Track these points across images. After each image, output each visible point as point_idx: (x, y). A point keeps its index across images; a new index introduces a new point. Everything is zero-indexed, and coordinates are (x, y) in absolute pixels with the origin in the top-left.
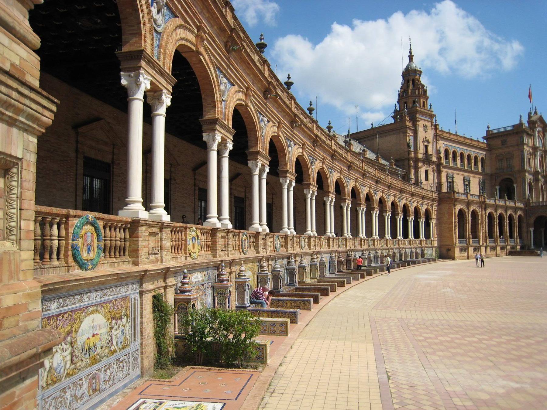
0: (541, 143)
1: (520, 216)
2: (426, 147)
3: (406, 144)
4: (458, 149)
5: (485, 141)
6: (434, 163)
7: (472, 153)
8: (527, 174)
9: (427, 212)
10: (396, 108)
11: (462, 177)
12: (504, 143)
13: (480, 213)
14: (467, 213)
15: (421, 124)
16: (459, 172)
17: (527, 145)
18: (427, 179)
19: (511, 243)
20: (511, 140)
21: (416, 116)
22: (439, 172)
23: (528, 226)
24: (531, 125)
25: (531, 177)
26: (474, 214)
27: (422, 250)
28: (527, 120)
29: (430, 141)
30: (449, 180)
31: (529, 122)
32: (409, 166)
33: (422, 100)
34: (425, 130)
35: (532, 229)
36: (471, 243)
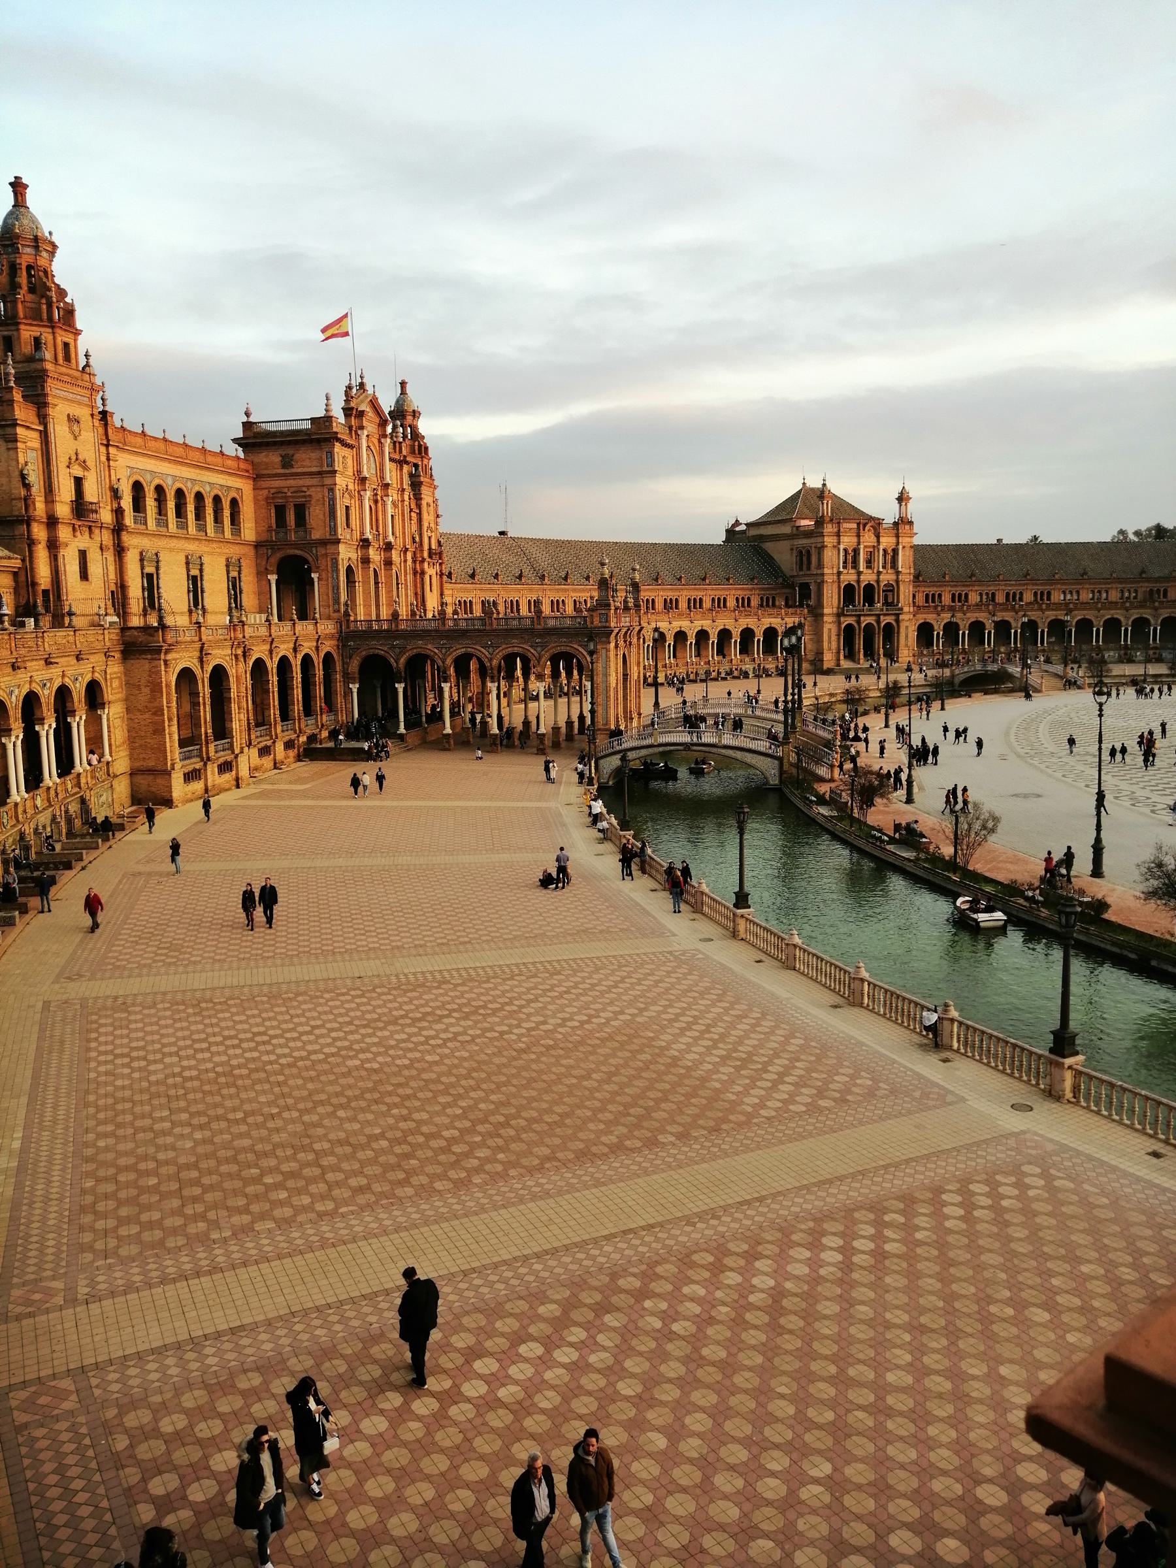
1: (328, 655)
2: (78, 482)
3: (17, 473)
4: (170, 481)
9: (94, 692)
12: (287, 462)
13: (232, 672)
14: (199, 677)
15: (59, 411)
16: (173, 543)
18: (84, 575)
19: (309, 727)
20: (307, 460)
21: (43, 387)
22: (120, 551)
23: (347, 678)
26: (219, 675)
27: (83, 801)
28: (343, 404)
29: (90, 463)
31: (348, 411)
32: (31, 543)
33: (59, 339)
35: (355, 687)
36: (212, 754)
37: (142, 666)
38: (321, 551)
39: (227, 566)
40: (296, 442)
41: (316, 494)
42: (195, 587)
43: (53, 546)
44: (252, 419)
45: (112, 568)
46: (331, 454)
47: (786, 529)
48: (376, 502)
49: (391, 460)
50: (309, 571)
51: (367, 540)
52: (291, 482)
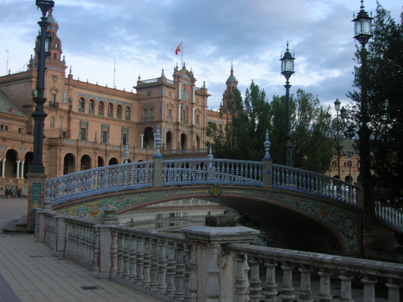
0: (187, 96)
4: (97, 98)
5: (135, 91)
6: (61, 110)
7: (115, 102)
10: (32, 58)
11: (100, 125)
12: (149, 94)
16: (96, 119)
17: (167, 97)
20: (155, 92)
22: (69, 119)
24: (176, 80)
29: (59, 90)
30: (82, 127)
31: (174, 76)
34: (53, 80)
37: (53, 150)
39: (122, 130)
40: (152, 87)
42: (105, 135)
44: (141, 80)
46: (162, 90)
48: (187, 109)
49: (196, 94)
50: (153, 133)
51: (179, 122)
52: (150, 101)
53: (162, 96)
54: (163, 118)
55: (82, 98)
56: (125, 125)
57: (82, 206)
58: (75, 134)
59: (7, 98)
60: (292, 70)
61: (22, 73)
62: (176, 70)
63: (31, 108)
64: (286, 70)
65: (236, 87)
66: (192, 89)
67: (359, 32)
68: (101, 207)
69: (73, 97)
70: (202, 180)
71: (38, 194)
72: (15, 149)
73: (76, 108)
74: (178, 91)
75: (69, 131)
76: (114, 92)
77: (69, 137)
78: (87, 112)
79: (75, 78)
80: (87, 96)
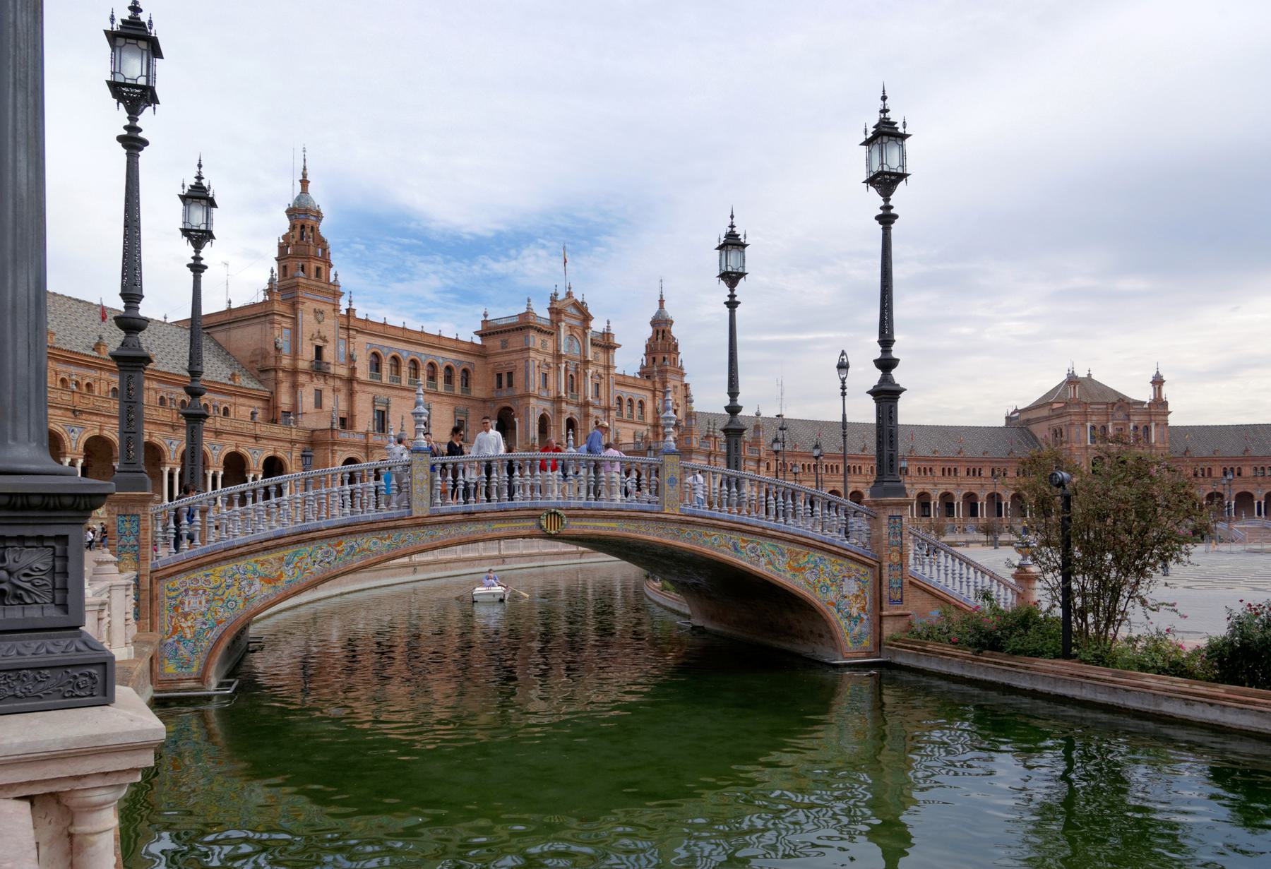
2: (319, 350)
4: (405, 354)
5: (478, 340)
6: (334, 377)
8: (532, 401)
12: (504, 344)
16: (405, 393)
17: (537, 351)
18: (319, 404)
20: (515, 341)
22: (351, 394)
24: (554, 317)
25: (547, 405)
32: (277, 383)
38: (521, 402)
41: (521, 364)
43: (295, 387)
45: (343, 406)
47: (1045, 412)
48: (577, 373)
49: (593, 344)
52: (506, 358)
53: (529, 349)
54: (531, 388)
55: (375, 355)
56: (462, 404)
57: (242, 564)
58: (364, 420)
59: (228, 353)
60: (740, 270)
61: (255, 305)
62: (553, 299)
63: (273, 373)
64: (729, 269)
65: (669, 332)
66: (585, 334)
67: (876, 168)
68: (288, 564)
69: (356, 353)
70: (580, 498)
71: (132, 540)
72: (242, 450)
73: (363, 372)
74: (558, 338)
75: (352, 416)
76: (438, 342)
77: (352, 427)
78: (386, 379)
79: (360, 314)
80: (386, 350)
